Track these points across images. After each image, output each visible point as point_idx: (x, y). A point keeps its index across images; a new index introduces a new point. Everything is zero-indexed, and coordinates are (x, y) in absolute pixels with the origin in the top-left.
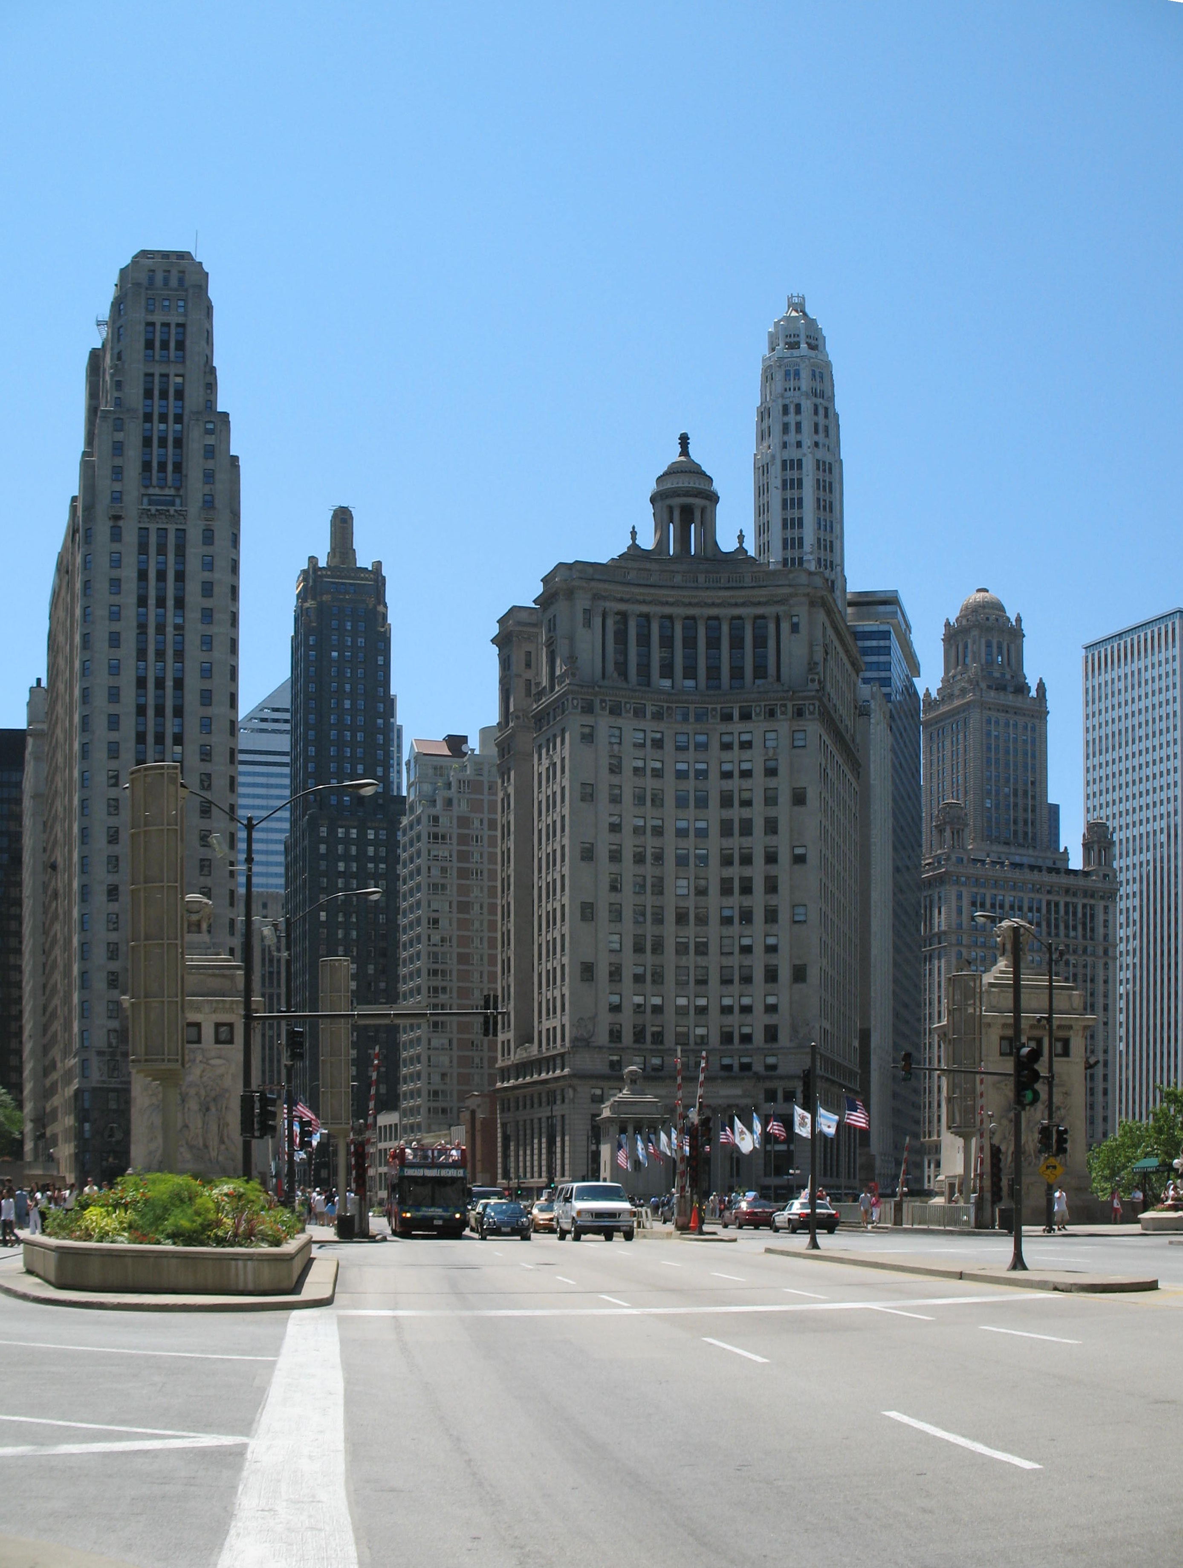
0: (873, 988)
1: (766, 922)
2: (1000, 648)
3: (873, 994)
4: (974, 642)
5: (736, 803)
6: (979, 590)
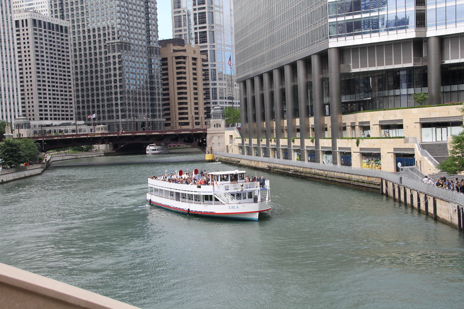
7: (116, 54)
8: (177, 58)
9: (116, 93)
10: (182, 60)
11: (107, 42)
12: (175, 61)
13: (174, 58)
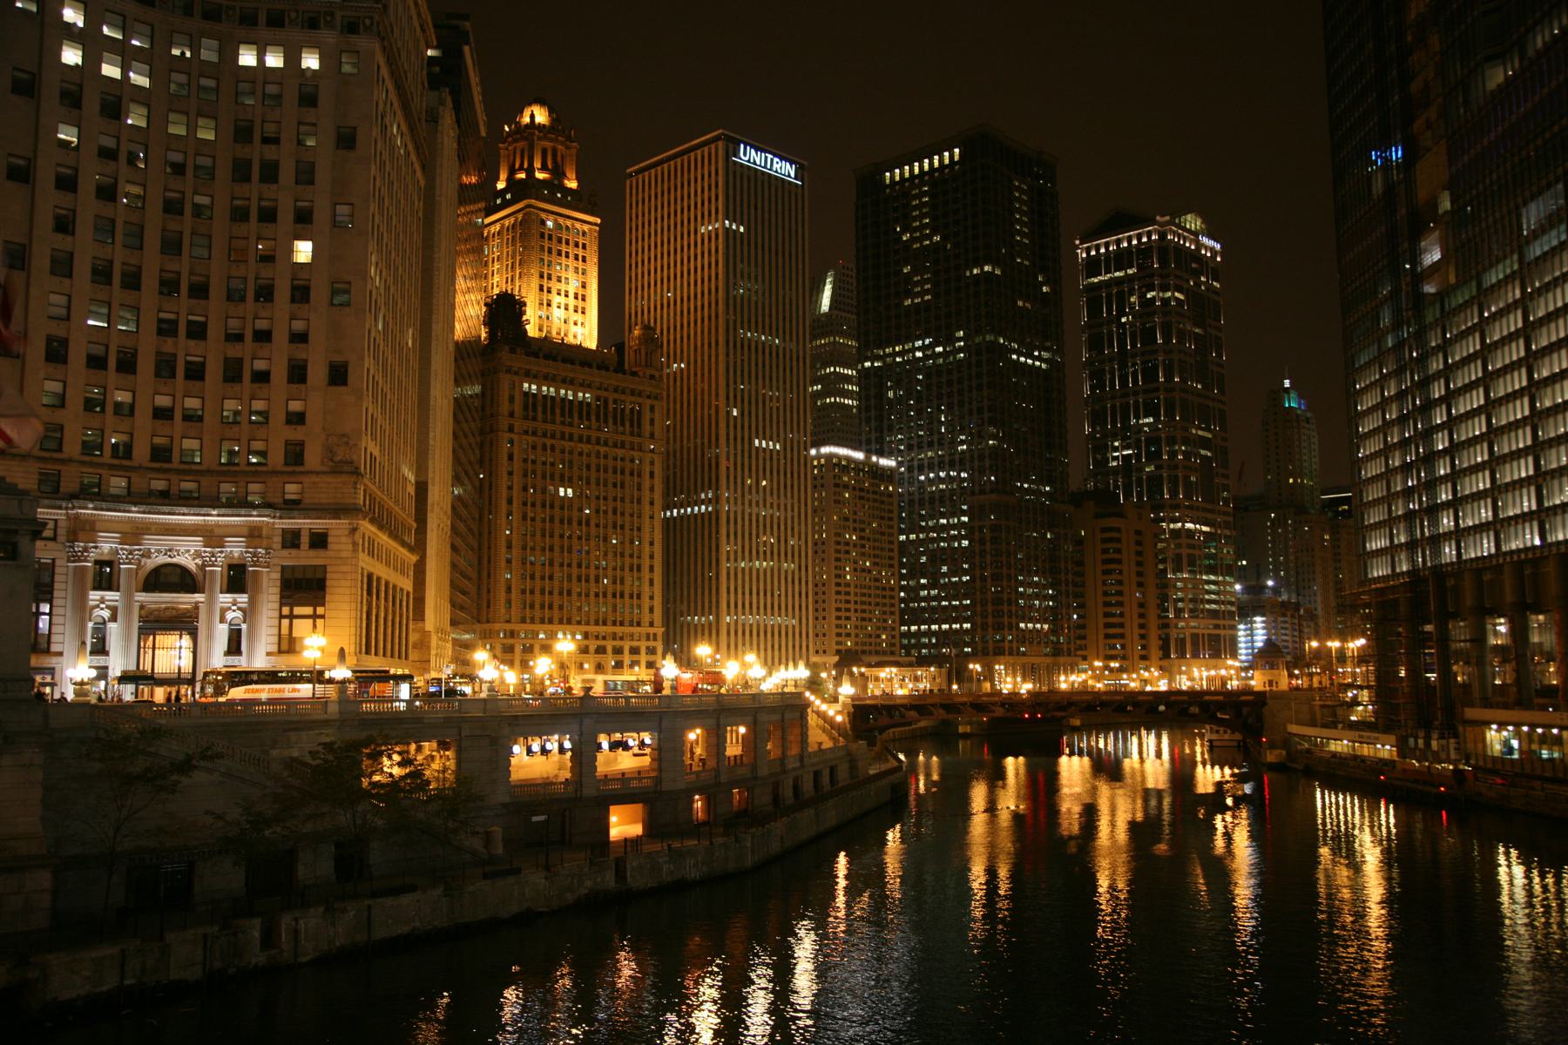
0: (431, 435)
1: (293, 300)
3: (431, 442)
5: (257, 138)
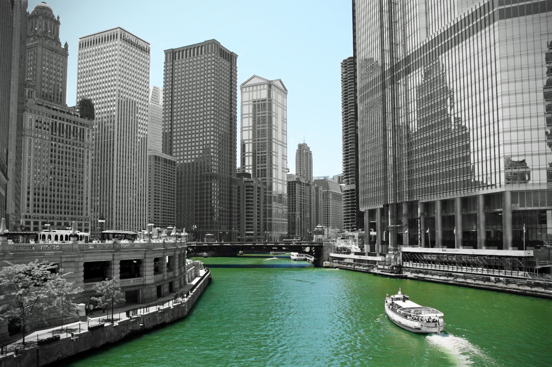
2: (51, 26)
4: (40, 21)
6: (42, 2)
7: (209, 182)
8: (247, 187)
9: (207, 210)
10: (251, 189)
11: (202, 173)
12: (245, 189)
13: (245, 187)
